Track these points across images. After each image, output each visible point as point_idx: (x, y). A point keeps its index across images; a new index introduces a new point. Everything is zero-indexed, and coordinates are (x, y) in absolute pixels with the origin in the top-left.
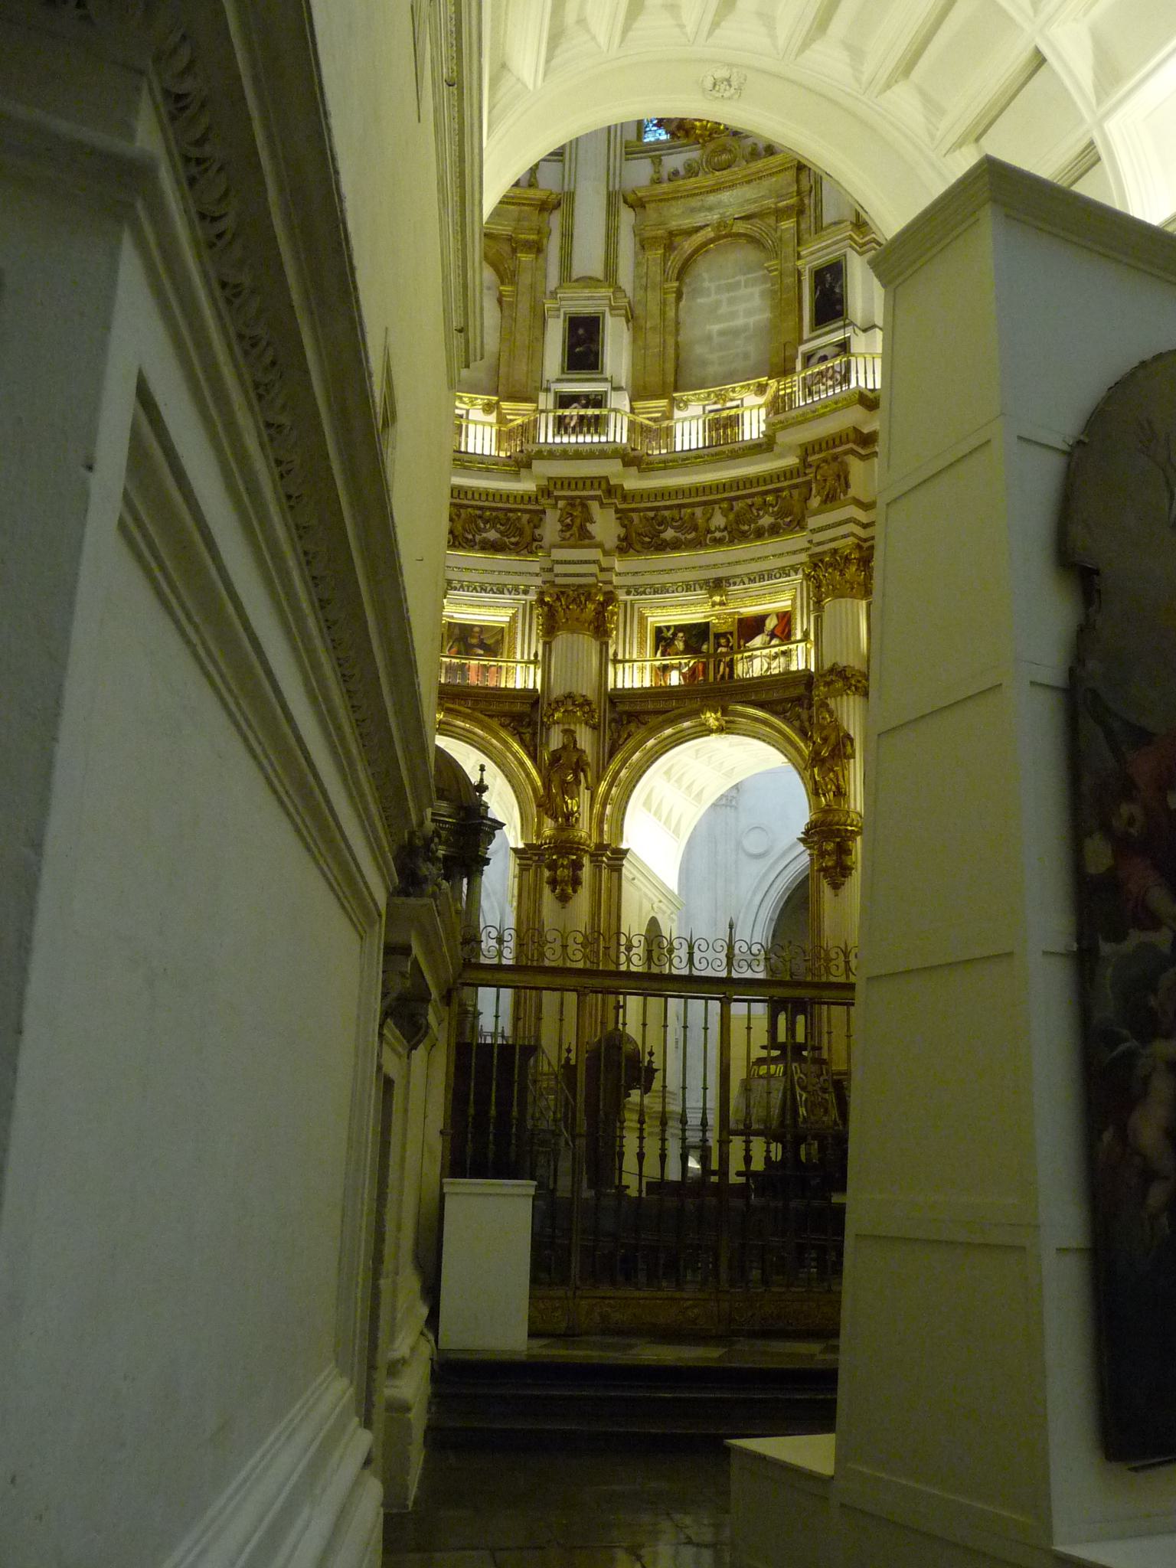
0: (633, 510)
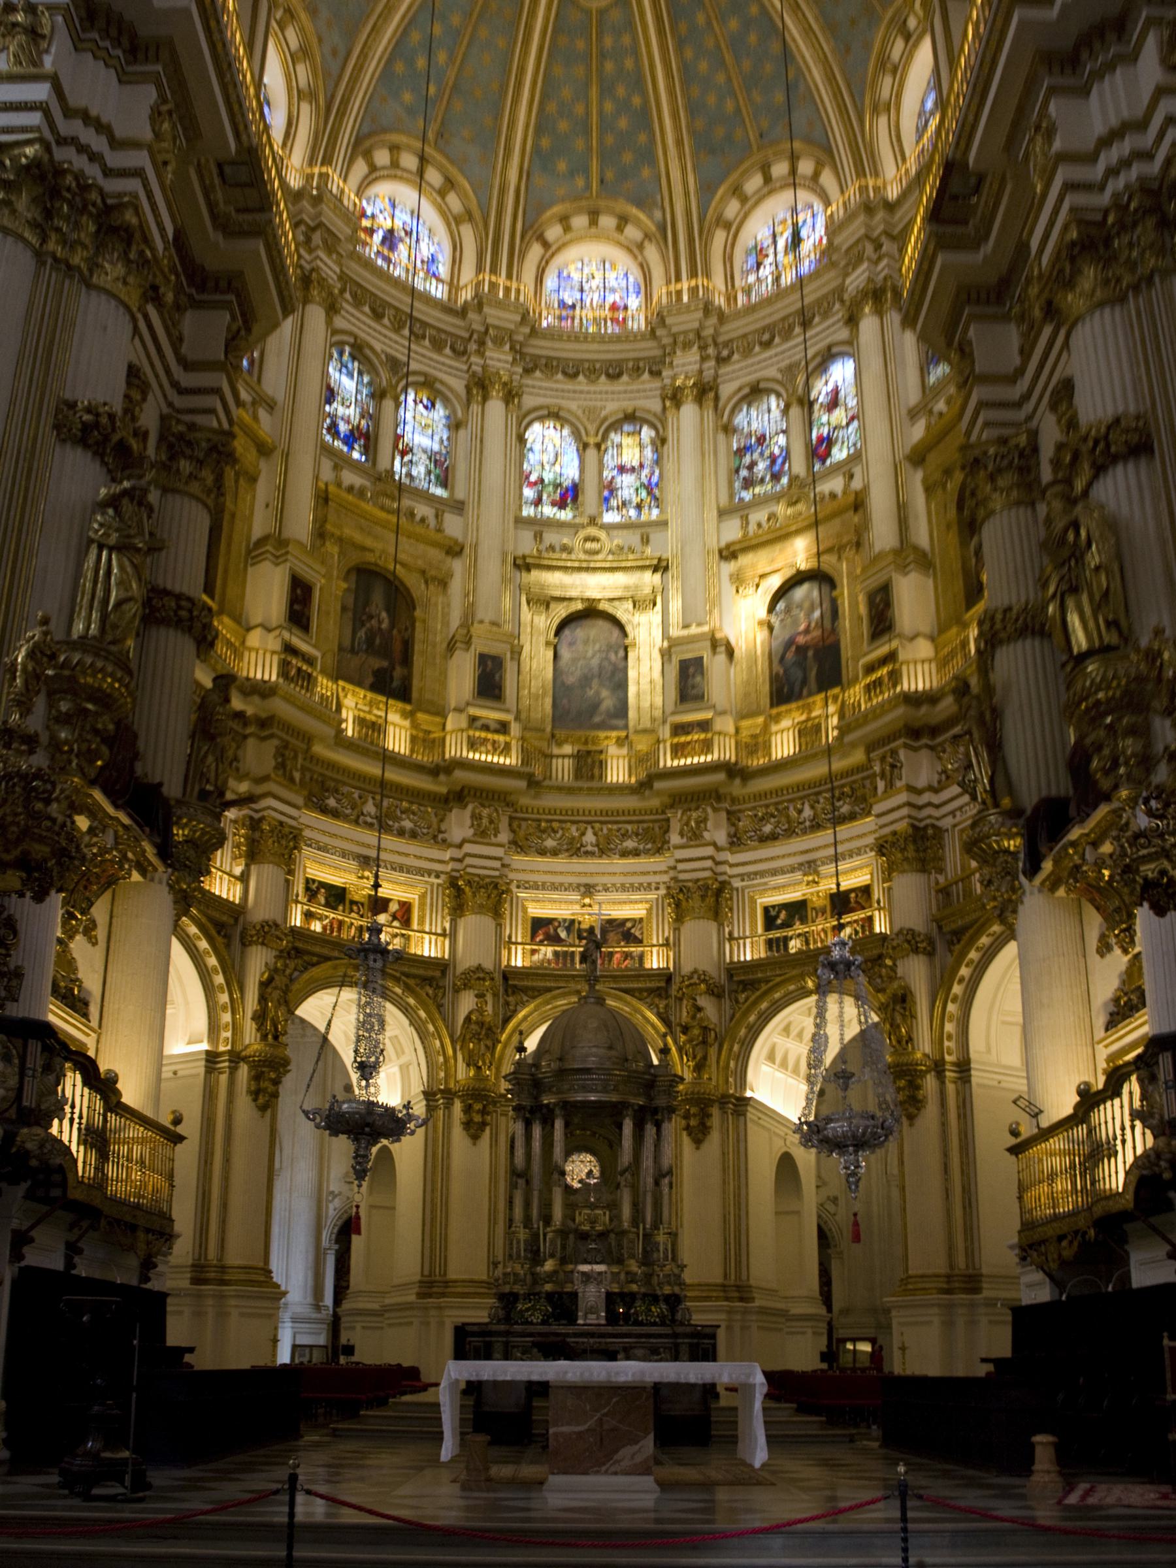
0: (740, 811)
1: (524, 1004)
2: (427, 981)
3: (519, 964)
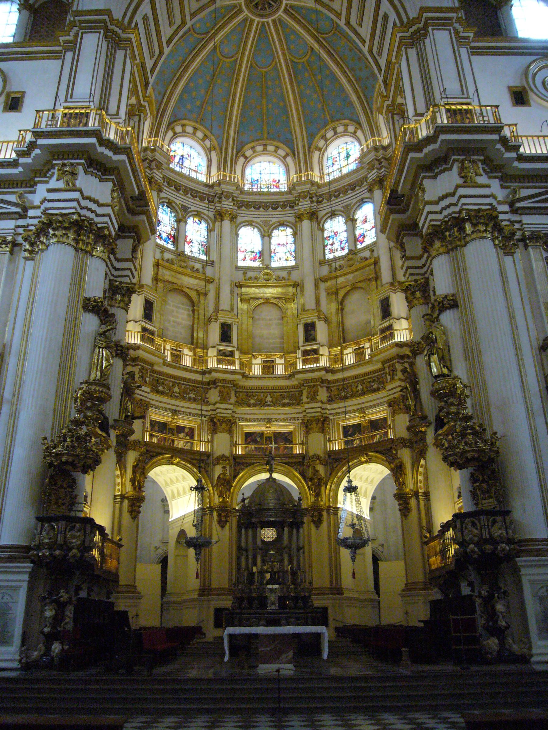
1: (243, 470)
2: (202, 461)
3: (240, 453)
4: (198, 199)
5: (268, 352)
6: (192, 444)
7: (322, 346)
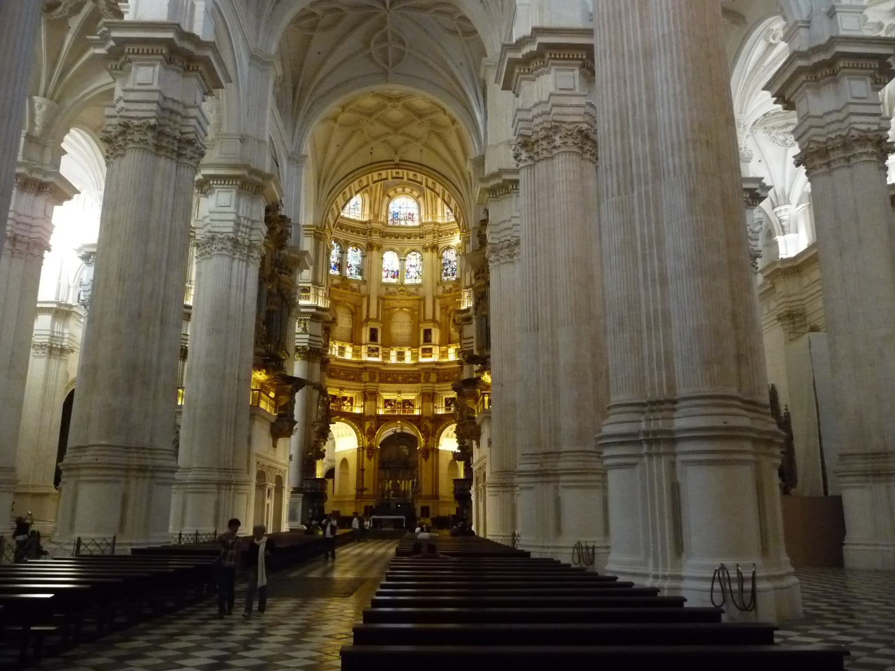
4: (355, 233)
5: (401, 345)
6: (352, 409)
7: (435, 345)
